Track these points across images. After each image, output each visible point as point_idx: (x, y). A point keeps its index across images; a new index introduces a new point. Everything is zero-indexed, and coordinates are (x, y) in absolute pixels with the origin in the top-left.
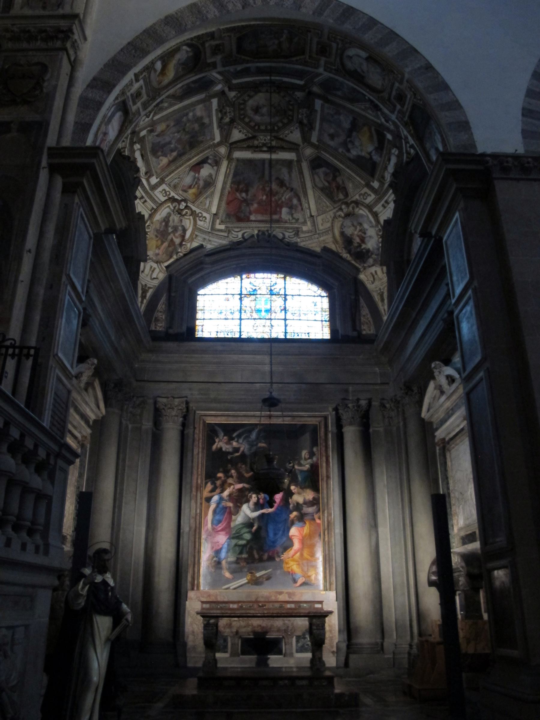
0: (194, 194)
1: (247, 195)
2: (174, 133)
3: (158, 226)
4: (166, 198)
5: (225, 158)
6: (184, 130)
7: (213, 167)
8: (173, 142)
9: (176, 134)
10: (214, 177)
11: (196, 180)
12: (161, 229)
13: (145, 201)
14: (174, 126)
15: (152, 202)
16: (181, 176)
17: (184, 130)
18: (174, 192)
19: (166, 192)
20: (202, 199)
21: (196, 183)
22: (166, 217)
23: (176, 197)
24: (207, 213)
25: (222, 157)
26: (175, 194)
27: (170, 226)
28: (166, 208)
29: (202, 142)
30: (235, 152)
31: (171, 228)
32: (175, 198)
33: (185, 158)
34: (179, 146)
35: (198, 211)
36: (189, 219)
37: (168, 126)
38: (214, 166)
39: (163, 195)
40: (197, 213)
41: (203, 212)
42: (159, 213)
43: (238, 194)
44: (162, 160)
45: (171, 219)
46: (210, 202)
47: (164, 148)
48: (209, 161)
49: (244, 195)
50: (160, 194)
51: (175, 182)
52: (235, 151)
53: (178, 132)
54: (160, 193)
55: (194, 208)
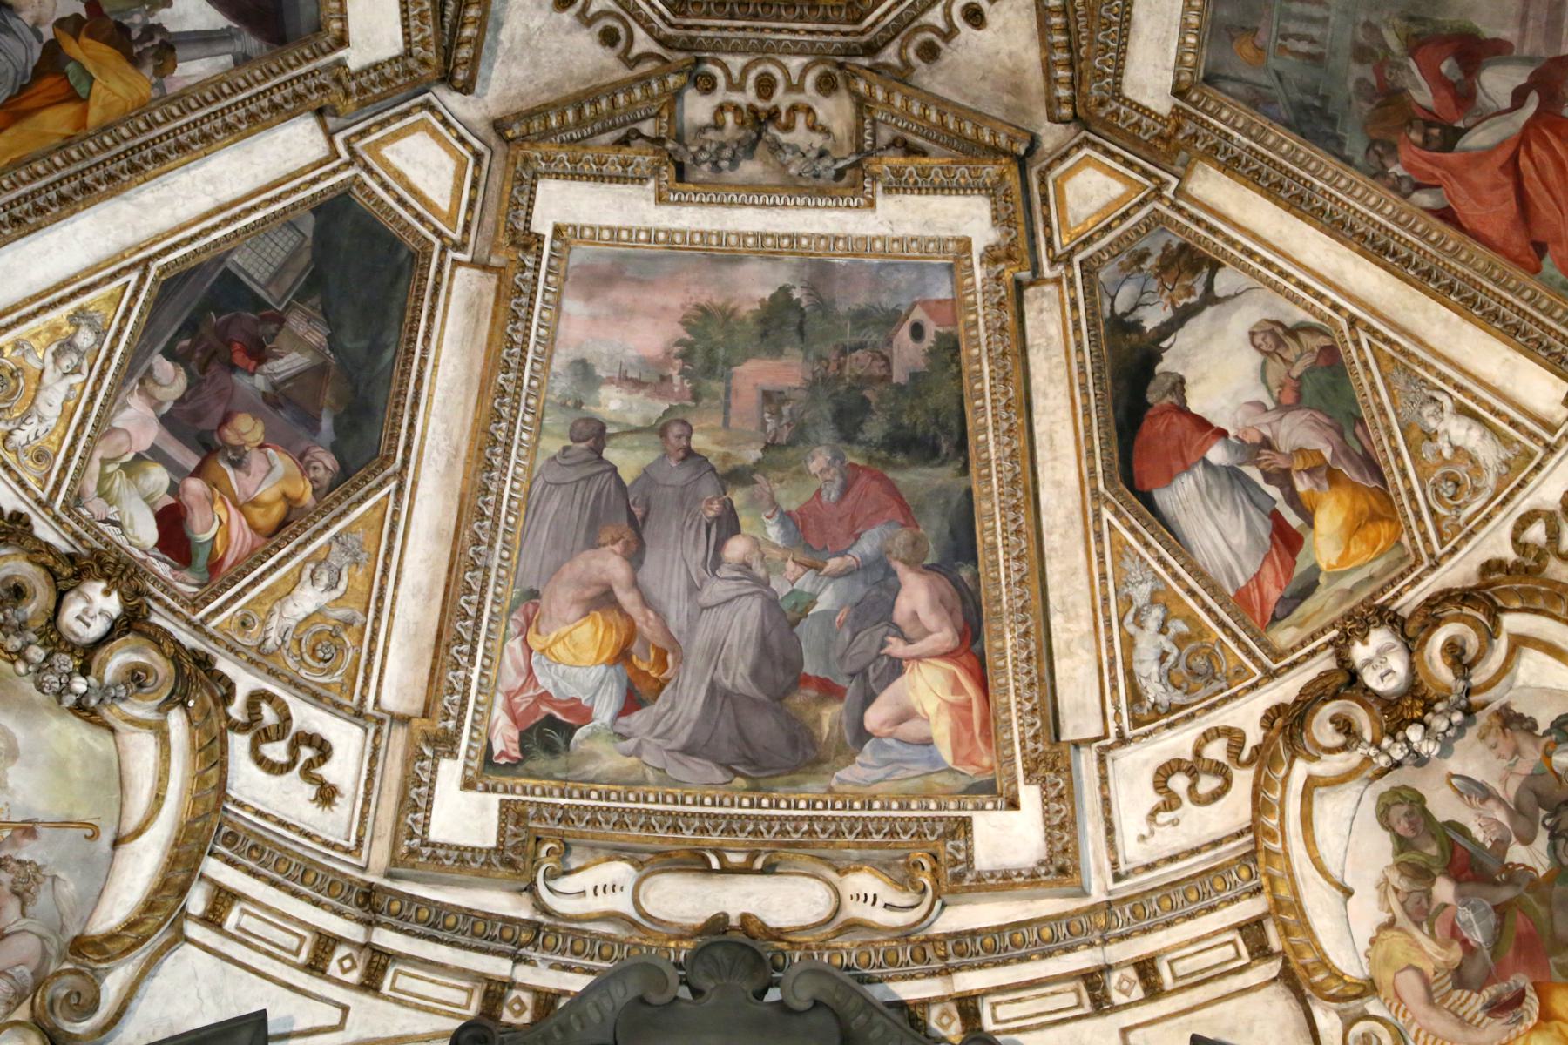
0: (1356, 527)
1: (1498, 50)
2: (715, 561)
3: (1429, 946)
4: (1243, 779)
5: (1164, 183)
6: (738, 476)
7: (1210, 298)
8: (790, 579)
9: (736, 548)
10: (1301, 315)
11: (1254, 474)
12: (1477, 936)
13: (1146, 968)
14: (635, 556)
15: (1191, 916)
16: (1141, 593)
17: (738, 476)
18: (1235, 696)
19: (1193, 771)
20: (1405, 476)
21: (1282, 478)
22: (1402, 844)
23: (1286, 689)
24: (1538, 467)
25: (1142, 203)
26: (1255, 686)
27: (1501, 845)
28: (1307, 820)
29: (949, 349)
30: (1128, 92)
31: (1527, 840)
32: (1290, 699)
33: (993, 527)
34: (867, 545)
35: (1496, 543)
36: (1519, 642)
37: (603, 600)
38: (1209, 286)
39: (1198, 801)
40: (1509, 554)
41: (1523, 503)
42: (1317, 899)
43: (1479, 139)
44: (907, 715)
45: (1444, 806)
46: (1461, 410)
47: (809, 669)
48: (1152, 318)
49: (1497, 83)
50: (1175, 823)
51: (1163, 657)
52: (1117, 94)
53: (728, 524)
54: (1163, 817)
55: (1458, 571)
